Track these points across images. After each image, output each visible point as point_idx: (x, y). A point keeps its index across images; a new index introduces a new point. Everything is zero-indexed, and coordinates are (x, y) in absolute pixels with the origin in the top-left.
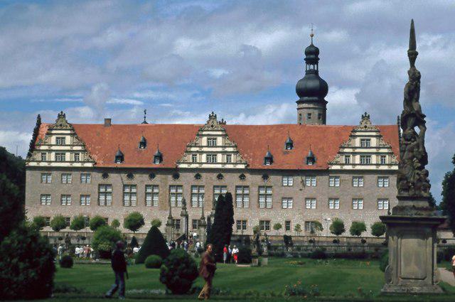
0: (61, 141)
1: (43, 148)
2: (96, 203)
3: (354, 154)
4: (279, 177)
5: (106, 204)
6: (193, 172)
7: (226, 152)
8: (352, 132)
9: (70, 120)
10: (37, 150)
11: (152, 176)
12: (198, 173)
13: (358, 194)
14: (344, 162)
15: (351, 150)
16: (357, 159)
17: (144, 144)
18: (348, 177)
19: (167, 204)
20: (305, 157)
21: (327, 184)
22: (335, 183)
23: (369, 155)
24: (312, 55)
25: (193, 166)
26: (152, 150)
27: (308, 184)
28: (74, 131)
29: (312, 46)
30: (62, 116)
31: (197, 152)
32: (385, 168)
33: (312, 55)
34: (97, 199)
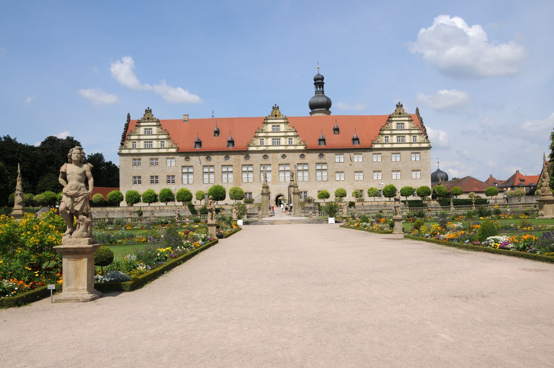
0: (148, 132)
1: (132, 137)
2: (180, 181)
3: (392, 135)
4: (332, 155)
5: (188, 182)
6: (261, 153)
7: (288, 136)
8: (389, 117)
9: (156, 114)
10: (128, 140)
11: (227, 158)
12: (265, 153)
13: (397, 166)
14: (384, 142)
15: (389, 132)
16: (394, 139)
17: (217, 132)
19: (240, 180)
21: (371, 159)
22: (376, 158)
24: (319, 82)
27: (356, 160)
28: (159, 124)
30: (148, 111)
31: (264, 137)
32: (417, 145)
33: (319, 82)
34: (180, 179)
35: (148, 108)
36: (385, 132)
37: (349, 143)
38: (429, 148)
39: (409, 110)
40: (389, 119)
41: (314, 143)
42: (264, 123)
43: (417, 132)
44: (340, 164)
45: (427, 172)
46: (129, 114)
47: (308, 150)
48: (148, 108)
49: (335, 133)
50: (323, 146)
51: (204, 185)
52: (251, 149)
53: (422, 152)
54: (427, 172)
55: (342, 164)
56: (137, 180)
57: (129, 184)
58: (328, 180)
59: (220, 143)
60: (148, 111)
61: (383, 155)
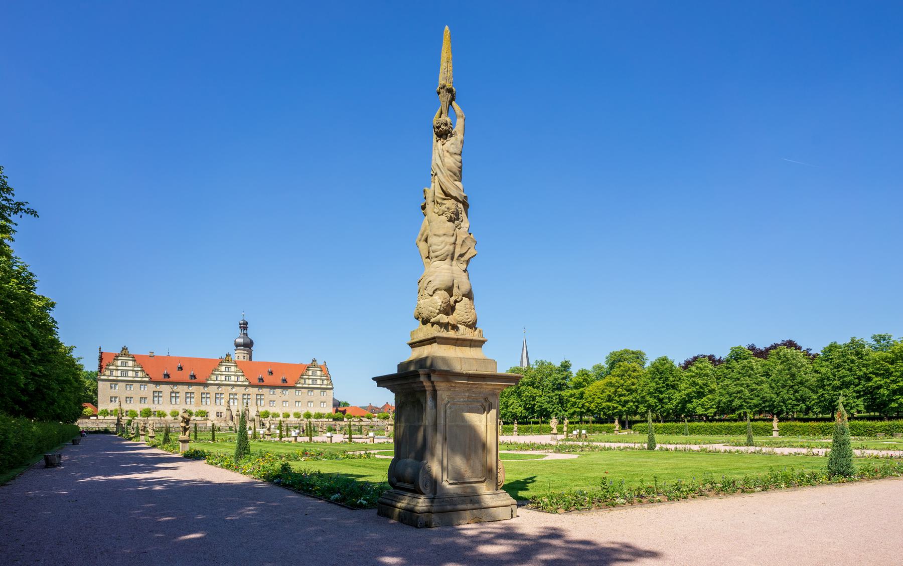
13: (311, 399)
15: (307, 377)
16: (310, 382)
23: (316, 379)
25: (217, 382)
31: (219, 374)
36: (304, 377)
38: (332, 389)
39: (320, 362)
40: (308, 368)
41: (256, 382)
42: (219, 365)
43: (325, 378)
47: (252, 385)
50: (262, 383)
52: (209, 382)
57: (107, 402)
59: (185, 376)
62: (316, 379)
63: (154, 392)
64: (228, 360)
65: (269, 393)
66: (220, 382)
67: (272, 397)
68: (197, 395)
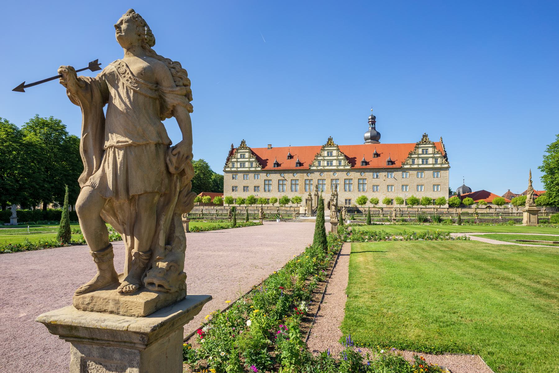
0: (243, 156)
2: (263, 190)
6: (319, 172)
9: (248, 144)
13: (421, 182)
16: (420, 161)
18: (415, 172)
19: (304, 190)
20: (387, 160)
23: (427, 159)
24: (373, 121)
26: (295, 160)
29: (372, 116)
30: (243, 142)
31: (321, 159)
33: (373, 121)
35: (243, 140)
37: (384, 164)
38: (447, 169)
39: (433, 138)
44: (377, 179)
45: (445, 187)
46: (232, 144)
48: (243, 140)
49: (374, 157)
51: (279, 193)
53: (442, 172)
54: (445, 187)
55: (378, 179)
56: (234, 189)
58: (367, 191)
60: (243, 142)
61: (410, 173)
62: (427, 159)
63: (265, 180)
64: (330, 144)
65: (371, 177)
66: (322, 168)
67: (376, 181)
68: (301, 183)
